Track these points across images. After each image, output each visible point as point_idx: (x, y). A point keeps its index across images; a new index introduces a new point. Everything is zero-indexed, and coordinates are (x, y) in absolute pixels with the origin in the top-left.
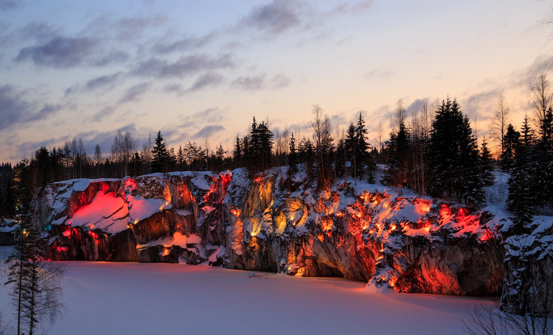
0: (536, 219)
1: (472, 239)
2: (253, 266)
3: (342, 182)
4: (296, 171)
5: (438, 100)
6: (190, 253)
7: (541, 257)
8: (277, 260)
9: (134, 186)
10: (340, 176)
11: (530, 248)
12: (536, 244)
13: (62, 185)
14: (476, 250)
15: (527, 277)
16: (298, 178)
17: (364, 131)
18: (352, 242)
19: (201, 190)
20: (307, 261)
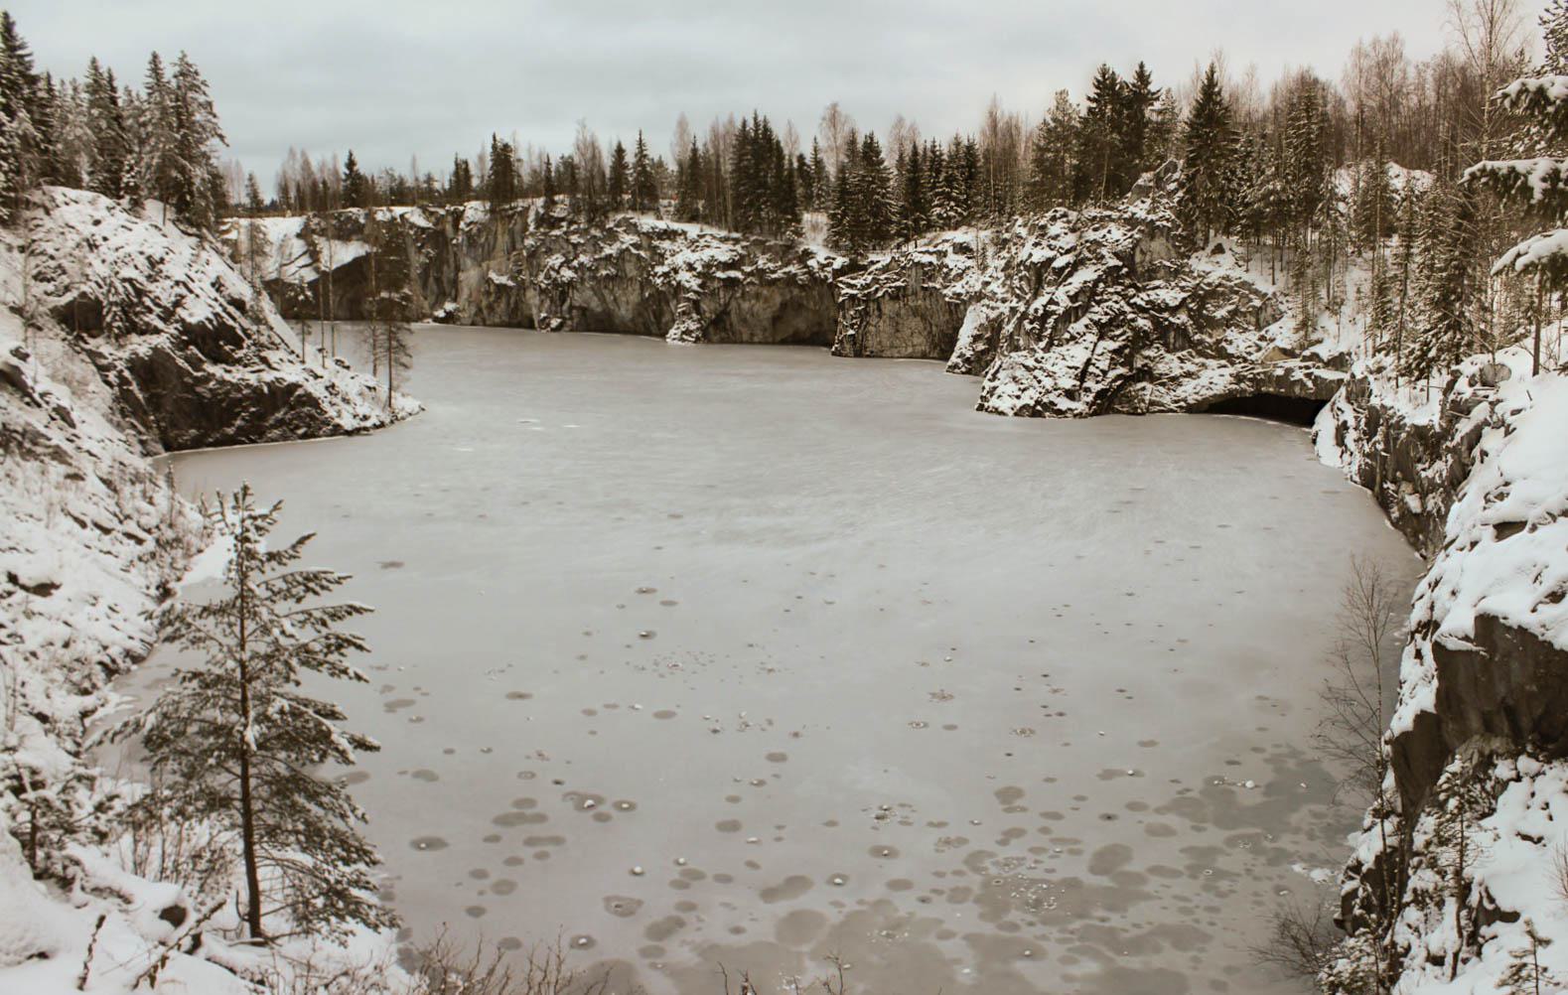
0: (872, 257)
1: (791, 279)
2: (497, 320)
3: (619, 217)
4: (555, 203)
5: (1045, 123)
7: (880, 294)
8: (534, 311)
9: (323, 224)
10: (616, 210)
11: (868, 286)
12: (876, 280)
14: (796, 291)
15: (866, 313)
16: (559, 212)
18: (637, 286)
19: (419, 228)
20: (575, 312)
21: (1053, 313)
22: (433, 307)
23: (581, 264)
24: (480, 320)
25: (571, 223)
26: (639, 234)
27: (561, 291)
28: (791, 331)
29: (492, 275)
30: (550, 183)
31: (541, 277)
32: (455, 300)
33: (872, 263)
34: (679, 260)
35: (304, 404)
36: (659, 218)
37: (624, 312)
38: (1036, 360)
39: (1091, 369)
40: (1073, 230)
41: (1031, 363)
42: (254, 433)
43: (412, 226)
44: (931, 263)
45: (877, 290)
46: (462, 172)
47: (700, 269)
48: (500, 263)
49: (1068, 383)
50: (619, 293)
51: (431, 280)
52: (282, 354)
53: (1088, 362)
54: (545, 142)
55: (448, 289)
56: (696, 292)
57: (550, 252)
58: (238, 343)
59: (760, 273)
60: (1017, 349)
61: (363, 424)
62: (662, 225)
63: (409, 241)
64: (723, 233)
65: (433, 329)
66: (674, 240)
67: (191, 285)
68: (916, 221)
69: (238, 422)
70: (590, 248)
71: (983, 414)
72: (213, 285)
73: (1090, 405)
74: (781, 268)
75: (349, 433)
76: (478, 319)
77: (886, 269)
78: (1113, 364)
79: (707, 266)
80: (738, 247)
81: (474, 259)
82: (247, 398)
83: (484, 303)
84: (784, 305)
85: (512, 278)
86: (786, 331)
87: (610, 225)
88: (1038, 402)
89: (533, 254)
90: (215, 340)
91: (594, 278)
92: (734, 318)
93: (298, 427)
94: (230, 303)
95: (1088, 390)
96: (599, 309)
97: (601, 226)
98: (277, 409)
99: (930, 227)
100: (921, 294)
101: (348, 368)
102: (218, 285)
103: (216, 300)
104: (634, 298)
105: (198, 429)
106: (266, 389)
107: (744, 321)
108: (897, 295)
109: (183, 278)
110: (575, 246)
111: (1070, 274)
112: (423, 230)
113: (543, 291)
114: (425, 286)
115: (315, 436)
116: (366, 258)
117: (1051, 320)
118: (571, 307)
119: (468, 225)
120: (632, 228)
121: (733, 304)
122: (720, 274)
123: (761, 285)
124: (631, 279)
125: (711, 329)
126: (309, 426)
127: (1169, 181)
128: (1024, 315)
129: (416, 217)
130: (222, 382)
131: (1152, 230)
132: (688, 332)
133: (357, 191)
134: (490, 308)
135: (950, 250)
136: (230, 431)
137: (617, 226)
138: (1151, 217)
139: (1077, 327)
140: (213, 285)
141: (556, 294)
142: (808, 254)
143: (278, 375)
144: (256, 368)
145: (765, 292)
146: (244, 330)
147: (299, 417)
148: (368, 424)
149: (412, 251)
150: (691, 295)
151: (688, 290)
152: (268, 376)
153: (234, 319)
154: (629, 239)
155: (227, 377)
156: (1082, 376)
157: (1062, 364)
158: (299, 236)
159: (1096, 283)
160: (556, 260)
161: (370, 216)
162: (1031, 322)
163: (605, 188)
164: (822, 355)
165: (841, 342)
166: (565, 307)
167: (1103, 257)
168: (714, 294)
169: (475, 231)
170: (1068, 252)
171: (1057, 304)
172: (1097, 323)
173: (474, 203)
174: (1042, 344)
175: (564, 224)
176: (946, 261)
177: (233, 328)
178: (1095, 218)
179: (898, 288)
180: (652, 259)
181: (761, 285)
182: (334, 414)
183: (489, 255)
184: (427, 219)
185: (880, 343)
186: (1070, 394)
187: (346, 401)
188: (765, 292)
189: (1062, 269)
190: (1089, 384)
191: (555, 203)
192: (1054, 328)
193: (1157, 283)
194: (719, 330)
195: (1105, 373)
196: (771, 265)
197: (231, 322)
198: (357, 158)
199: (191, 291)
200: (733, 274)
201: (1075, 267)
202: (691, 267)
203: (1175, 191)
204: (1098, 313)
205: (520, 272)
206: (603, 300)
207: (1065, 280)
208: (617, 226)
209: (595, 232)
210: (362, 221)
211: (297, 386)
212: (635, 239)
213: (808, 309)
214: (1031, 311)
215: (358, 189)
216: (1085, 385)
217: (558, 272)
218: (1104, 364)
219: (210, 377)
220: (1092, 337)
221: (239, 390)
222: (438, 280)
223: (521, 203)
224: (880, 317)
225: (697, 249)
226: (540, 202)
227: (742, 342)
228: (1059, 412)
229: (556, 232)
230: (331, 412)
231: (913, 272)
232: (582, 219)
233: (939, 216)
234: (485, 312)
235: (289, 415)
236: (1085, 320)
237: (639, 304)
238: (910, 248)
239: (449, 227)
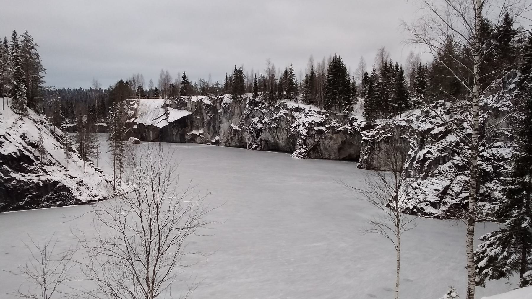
0: (378, 122)
1: (346, 131)
2: (234, 144)
3: (281, 102)
4: (258, 95)
6: (201, 138)
7: (379, 140)
8: (247, 141)
10: (280, 99)
11: (374, 136)
13: (133, 101)
14: (348, 137)
15: (372, 150)
16: (258, 99)
17: (293, 75)
21: (429, 158)
22: (212, 138)
23: (265, 122)
24: (228, 144)
25: (263, 104)
26: (287, 109)
27: (257, 133)
28: (347, 154)
29: (233, 125)
30: (256, 89)
31: (250, 127)
32: (219, 135)
33: (377, 125)
34: (300, 122)
35: (61, 190)
36: (296, 102)
37: (282, 143)
38: (418, 184)
39: (449, 192)
40: (447, 113)
41: (415, 185)
42: (35, 203)
43: (205, 104)
44: (405, 126)
45: (378, 138)
46: (228, 81)
47: (307, 125)
48: (236, 121)
49: (433, 198)
50: (279, 134)
51: (211, 127)
52: (56, 168)
53: (447, 188)
54: (255, 69)
55: (216, 132)
56: (305, 136)
57: (254, 116)
58: (31, 163)
59: (333, 128)
60: (410, 176)
61: (93, 199)
62: (296, 105)
63: (203, 110)
64: (318, 109)
65: (211, 148)
66: (300, 112)
67: (8, 137)
68: (400, 105)
69: (26, 199)
70: (269, 115)
71: (389, 209)
72: (21, 137)
73: (446, 212)
74: (342, 126)
75: (84, 203)
76: (227, 143)
77: (383, 128)
78: (464, 189)
79: (310, 124)
80: (324, 116)
81: (226, 118)
82: (31, 188)
83: (230, 137)
84: (343, 143)
85: (240, 127)
86: (345, 154)
87: (277, 105)
88: (415, 207)
89: (247, 117)
90: (19, 162)
91: (270, 128)
92: (322, 147)
93: (57, 201)
94: (29, 145)
95: (445, 203)
96: (272, 141)
97: (273, 105)
98: (48, 193)
99: (408, 107)
100: (399, 141)
101: (101, 172)
102: (23, 137)
103: (21, 144)
104: (285, 137)
105: (5, 202)
106: (42, 184)
107: (326, 149)
108: (387, 141)
109: (4, 134)
110: (264, 114)
111: (443, 137)
112: (209, 106)
113: (250, 133)
114: (209, 129)
115: (66, 205)
116: (188, 116)
117: (428, 162)
118: (261, 140)
119: (225, 104)
120: (285, 107)
121: (321, 141)
122: (315, 128)
123: (333, 133)
124: (284, 129)
125: (311, 152)
126: (63, 200)
127: (510, 83)
128: (414, 159)
129: (206, 100)
130: (19, 181)
131: (497, 113)
132: (300, 153)
133: (186, 89)
134: (232, 139)
135: (415, 119)
136: (22, 203)
137: (280, 106)
138: (495, 105)
139: (445, 167)
140: (21, 137)
141: (255, 134)
142: (354, 120)
143: (49, 177)
144: (39, 174)
145: (334, 136)
146: (36, 157)
147: (58, 196)
148: (96, 199)
149: (204, 114)
150: (303, 137)
151: (302, 135)
152: (43, 178)
153: (30, 152)
154: (283, 111)
155: (22, 179)
156: (443, 194)
157: (431, 186)
158: (162, 107)
159: (457, 144)
160: (256, 120)
161: (189, 99)
162: (417, 163)
163: (278, 88)
164: (350, 168)
165: (361, 162)
166: (259, 140)
167: (464, 128)
168: (312, 136)
169: (227, 106)
170: (442, 125)
171: (432, 154)
172: (457, 166)
173: (227, 95)
174: (421, 176)
175: (260, 104)
176: (412, 125)
177: (28, 157)
178: (463, 106)
179: (387, 137)
180: (292, 120)
181: (333, 133)
182: (78, 194)
183: (232, 117)
184: (211, 101)
185: (379, 163)
186: (434, 205)
187: (88, 189)
188: (334, 136)
189: (437, 135)
190: (447, 200)
191: (258, 95)
192: (429, 167)
193: (499, 144)
194: (315, 153)
195: (458, 195)
196: (337, 124)
197: (28, 154)
198: (187, 74)
199: (7, 140)
200: (321, 128)
201: (446, 134)
202: (304, 125)
203: (515, 89)
204: (457, 160)
205: (242, 124)
206: (273, 137)
207: (439, 140)
208: (280, 106)
209: (271, 108)
210: (187, 101)
211: (58, 182)
212: (286, 111)
213: (355, 145)
214: (417, 157)
215: (187, 88)
216: (445, 200)
217: (256, 125)
218: (458, 189)
219: (13, 179)
220: (452, 174)
221: (28, 185)
222: (214, 127)
223: (244, 96)
224: (380, 151)
225: (309, 116)
226: (251, 95)
227: (325, 159)
228: (426, 214)
229: (257, 108)
230: (76, 194)
231: (395, 130)
232: (267, 102)
233: (415, 102)
234: (230, 141)
235: (55, 195)
236: (449, 164)
237: (286, 140)
238: (398, 117)
239: (218, 105)
